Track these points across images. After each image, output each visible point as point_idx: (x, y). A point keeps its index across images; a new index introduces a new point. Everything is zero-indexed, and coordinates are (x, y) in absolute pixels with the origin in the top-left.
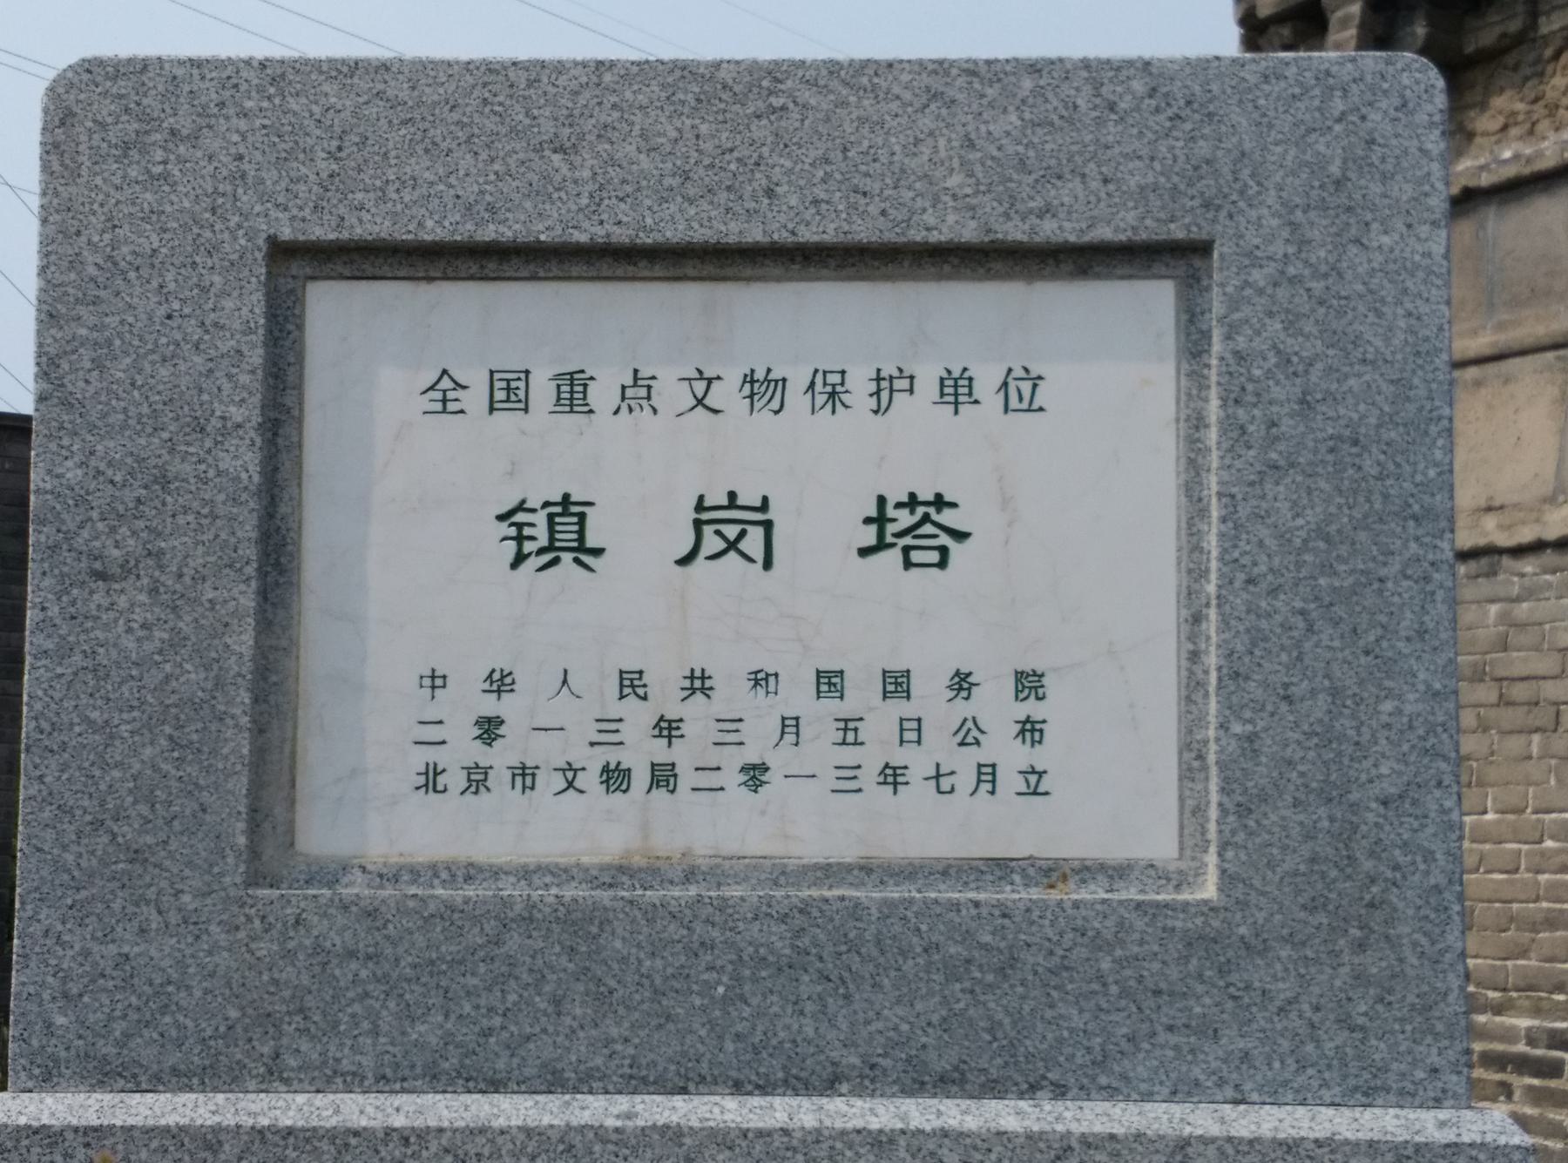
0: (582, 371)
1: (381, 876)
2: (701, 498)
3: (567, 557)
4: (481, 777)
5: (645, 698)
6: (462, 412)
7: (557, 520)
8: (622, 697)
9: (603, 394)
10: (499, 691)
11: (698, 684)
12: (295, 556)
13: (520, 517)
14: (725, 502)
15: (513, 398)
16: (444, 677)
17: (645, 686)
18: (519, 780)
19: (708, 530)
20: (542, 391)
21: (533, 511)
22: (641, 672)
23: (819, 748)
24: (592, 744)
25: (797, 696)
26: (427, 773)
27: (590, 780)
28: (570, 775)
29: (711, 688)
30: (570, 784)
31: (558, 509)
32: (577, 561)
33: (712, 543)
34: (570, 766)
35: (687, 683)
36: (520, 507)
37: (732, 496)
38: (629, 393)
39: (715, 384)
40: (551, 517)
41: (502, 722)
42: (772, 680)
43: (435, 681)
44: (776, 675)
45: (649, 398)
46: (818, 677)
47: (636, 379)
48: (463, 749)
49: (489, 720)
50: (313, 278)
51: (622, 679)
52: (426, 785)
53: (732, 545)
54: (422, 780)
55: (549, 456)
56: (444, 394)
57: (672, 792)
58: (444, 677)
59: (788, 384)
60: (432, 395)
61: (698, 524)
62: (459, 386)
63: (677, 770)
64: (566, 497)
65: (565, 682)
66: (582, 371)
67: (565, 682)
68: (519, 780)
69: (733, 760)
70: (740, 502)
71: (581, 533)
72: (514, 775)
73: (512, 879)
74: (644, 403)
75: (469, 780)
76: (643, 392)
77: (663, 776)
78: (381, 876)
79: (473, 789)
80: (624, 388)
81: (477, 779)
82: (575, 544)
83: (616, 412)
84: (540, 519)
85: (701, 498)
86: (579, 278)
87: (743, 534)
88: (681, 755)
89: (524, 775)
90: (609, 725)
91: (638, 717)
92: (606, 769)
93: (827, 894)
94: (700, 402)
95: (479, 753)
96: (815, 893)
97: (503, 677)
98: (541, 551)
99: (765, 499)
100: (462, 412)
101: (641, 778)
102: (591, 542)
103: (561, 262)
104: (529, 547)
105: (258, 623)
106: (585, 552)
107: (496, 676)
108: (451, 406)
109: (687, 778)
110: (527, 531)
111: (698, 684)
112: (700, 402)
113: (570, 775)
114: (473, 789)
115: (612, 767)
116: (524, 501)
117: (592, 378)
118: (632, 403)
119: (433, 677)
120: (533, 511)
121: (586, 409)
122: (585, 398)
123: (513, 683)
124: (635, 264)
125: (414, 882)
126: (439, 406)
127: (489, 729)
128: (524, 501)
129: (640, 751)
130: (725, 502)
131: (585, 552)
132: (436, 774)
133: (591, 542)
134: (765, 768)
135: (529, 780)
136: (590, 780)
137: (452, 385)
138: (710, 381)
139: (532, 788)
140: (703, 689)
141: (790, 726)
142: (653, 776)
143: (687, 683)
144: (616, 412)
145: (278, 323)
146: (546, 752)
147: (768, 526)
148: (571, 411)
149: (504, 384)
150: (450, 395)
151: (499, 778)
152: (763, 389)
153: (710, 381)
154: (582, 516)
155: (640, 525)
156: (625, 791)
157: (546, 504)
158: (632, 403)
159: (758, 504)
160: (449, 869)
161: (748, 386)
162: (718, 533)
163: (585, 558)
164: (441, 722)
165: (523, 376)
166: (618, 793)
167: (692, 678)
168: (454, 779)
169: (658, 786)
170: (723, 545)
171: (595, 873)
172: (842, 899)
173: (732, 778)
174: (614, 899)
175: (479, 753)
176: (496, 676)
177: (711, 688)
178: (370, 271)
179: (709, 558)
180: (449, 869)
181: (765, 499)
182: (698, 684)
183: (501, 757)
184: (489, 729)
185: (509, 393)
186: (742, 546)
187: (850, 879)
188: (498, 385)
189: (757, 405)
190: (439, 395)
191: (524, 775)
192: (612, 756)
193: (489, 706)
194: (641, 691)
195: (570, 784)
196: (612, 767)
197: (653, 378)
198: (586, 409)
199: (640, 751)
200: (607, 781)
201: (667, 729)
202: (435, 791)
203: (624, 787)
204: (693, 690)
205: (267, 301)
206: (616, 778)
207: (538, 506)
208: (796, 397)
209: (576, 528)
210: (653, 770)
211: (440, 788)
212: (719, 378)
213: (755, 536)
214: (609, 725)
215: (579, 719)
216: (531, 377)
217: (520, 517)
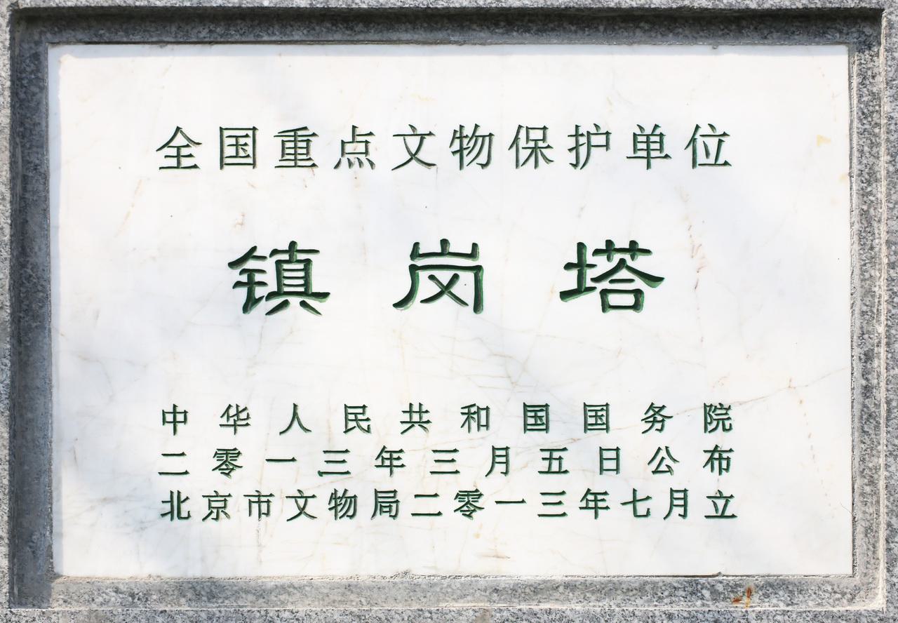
0: (305, 128)
1: (132, 595)
2: (416, 245)
3: (295, 301)
4: (221, 504)
5: (368, 430)
6: (195, 166)
7: (286, 266)
8: (347, 431)
9: (324, 151)
10: (235, 425)
11: (416, 418)
12: (45, 299)
13: (251, 264)
14: (439, 250)
15: (242, 153)
16: (185, 412)
17: (368, 419)
18: (255, 506)
19: (423, 275)
20: (269, 148)
21: (263, 258)
22: (364, 407)
23: (527, 478)
24: (321, 474)
25: (507, 427)
26: (171, 501)
27: (319, 506)
28: (301, 502)
29: (428, 422)
30: (302, 511)
31: (286, 257)
32: (303, 304)
33: (427, 288)
34: (720, 495)
35: (406, 417)
36: (250, 254)
37: (444, 243)
38: (349, 148)
39: (428, 139)
40: (279, 263)
41: (239, 453)
42: (483, 413)
43: (175, 418)
44: (487, 409)
45: (366, 153)
46: (525, 411)
47: (354, 135)
48: (202, 480)
49: (227, 452)
50: (54, 44)
51: (347, 414)
52: (172, 512)
53: (445, 289)
54: (167, 507)
55: (274, 205)
56: (178, 151)
57: (394, 517)
58: (185, 412)
59: (494, 139)
60: (167, 151)
61: (413, 269)
62: (191, 142)
63: (398, 498)
64: (293, 244)
65: (295, 415)
66: (305, 128)
67: (295, 415)
68: (255, 506)
69: (449, 487)
70: (452, 249)
71: (307, 278)
72: (250, 502)
73: (251, 597)
74: (362, 157)
75: (210, 507)
76: (361, 148)
77: (386, 503)
78: (132, 595)
79: (214, 515)
80: (343, 143)
81: (218, 506)
82: (302, 289)
83: (337, 166)
84: (269, 265)
85: (416, 245)
86: (408, 42)
87: (456, 277)
88: (404, 483)
89: (259, 502)
90: (336, 456)
91: (363, 448)
92: (334, 496)
93: (536, 608)
94: (413, 156)
95: (219, 483)
96: (524, 607)
97: (238, 413)
98: (271, 295)
99: (475, 246)
100: (195, 166)
101: (366, 504)
102: (315, 288)
103: (283, 27)
104: (259, 292)
105: (13, 363)
106: (310, 295)
107: (233, 411)
108: (186, 162)
109: (408, 504)
110: (258, 277)
111: (416, 418)
112: (413, 156)
113: (301, 502)
114: (214, 515)
115: (340, 494)
116: (254, 249)
117: (314, 135)
118: (352, 157)
119: (175, 413)
120: (263, 258)
121: (309, 163)
122: (308, 153)
123: (248, 417)
124: (352, 29)
125: (160, 601)
126: (173, 162)
127: (227, 460)
128: (254, 249)
129: (365, 481)
130: (439, 250)
131: (310, 295)
132: (179, 502)
133: (315, 288)
134: (477, 494)
135: (264, 507)
136: (319, 506)
137: (186, 142)
138: (422, 137)
139: (267, 514)
140: (421, 423)
141: (501, 456)
142: (376, 502)
143: (406, 417)
144: (337, 166)
145: (22, 86)
146: (281, 482)
147: (477, 269)
148: (295, 166)
149: (233, 141)
150: (184, 151)
151: (238, 505)
152: (471, 144)
153: (422, 137)
154: (307, 262)
155: (523, 274)
156: (351, 517)
157: (275, 252)
158: (352, 157)
159: (469, 251)
160: (193, 588)
161: (457, 142)
162: (432, 277)
163: (310, 301)
164: (183, 454)
165: (250, 133)
166: (345, 518)
167: (410, 412)
168: (197, 507)
169: (381, 512)
170: (437, 290)
171: (326, 591)
172: (549, 612)
173: (448, 503)
174: (344, 613)
175: (219, 483)
176: (233, 411)
177: (428, 422)
178: (107, 36)
179: (422, 302)
180: (193, 588)
181: (475, 246)
182: (416, 417)
183: (239, 486)
184: (227, 460)
185: (238, 147)
186: (455, 290)
187: (557, 595)
188: (228, 141)
189: (467, 160)
190: (173, 152)
191: (260, 502)
192: (340, 484)
193: (227, 439)
194: (364, 425)
195: (302, 511)
196: (340, 494)
197: (371, 134)
198: (309, 163)
199: (365, 481)
200: (335, 507)
201: (389, 459)
202: (180, 517)
203: (350, 513)
204: (412, 424)
205: (12, 65)
206: (343, 504)
207: (268, 255)
208: (502, 153)
209: (302, 274)
210: (376, 497)
211: (184, 514)
212: (430, 134)
213: (467, 278)
214: (336, 456)
215: (309, 450)
216: (257, 133)
217: (251, 264)
